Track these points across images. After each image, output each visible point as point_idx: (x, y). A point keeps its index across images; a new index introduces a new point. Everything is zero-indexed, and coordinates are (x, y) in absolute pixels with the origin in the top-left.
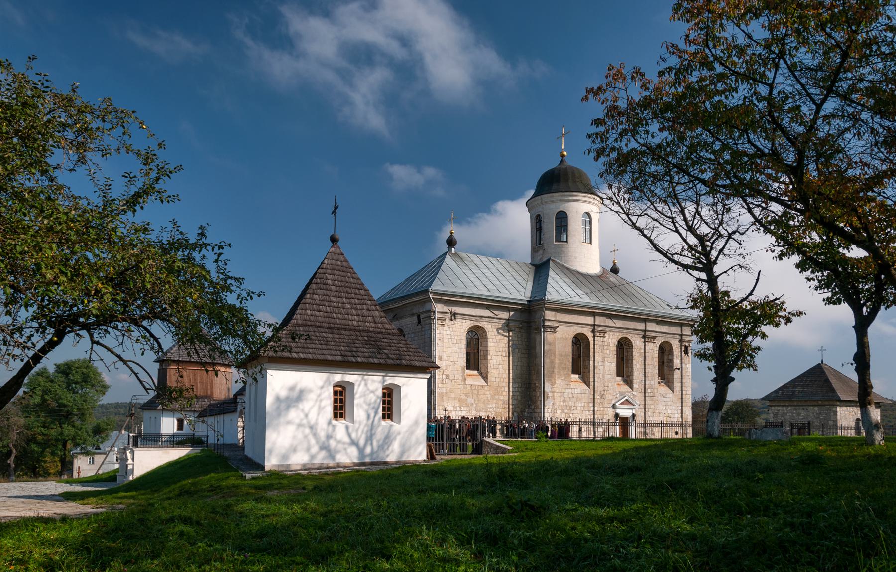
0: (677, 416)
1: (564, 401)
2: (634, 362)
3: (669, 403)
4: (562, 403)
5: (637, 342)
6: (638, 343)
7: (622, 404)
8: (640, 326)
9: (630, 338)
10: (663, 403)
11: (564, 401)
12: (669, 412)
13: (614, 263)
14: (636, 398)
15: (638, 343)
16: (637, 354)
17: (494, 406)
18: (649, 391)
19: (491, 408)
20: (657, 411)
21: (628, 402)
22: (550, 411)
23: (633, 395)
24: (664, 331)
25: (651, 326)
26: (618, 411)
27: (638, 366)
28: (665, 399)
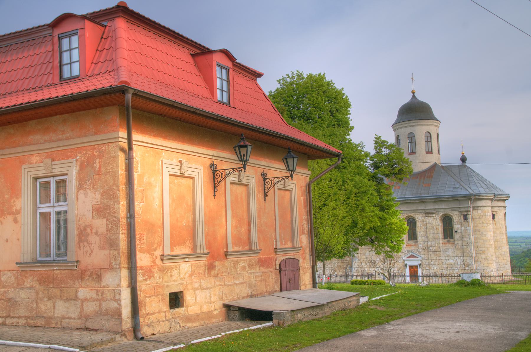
0: (459, 263)
1: (367, 258)
2: (418, 230)
3: (451, 255)
4: (365, 260)
5: (419, 218)
6: (420, 218)
7: (409, 257)
8: (421, 207)
9: (413, 216)
10: (446, 255)
11: (367, 258)
12: (451, 261)
13: (463, 154)
14: (421, 254)
15: (420, 218)
16: (419, 225)
17: (336, 262)
18: (431, 248)
19: (335, 263)
20: (441, 261)
21: (412, 256)
22: (356, 264)
23: (419, 251)
24: (443, 207)
25: (430, 207)
26: (406, 262)
27: (422, 233)
28: (447, 253)
